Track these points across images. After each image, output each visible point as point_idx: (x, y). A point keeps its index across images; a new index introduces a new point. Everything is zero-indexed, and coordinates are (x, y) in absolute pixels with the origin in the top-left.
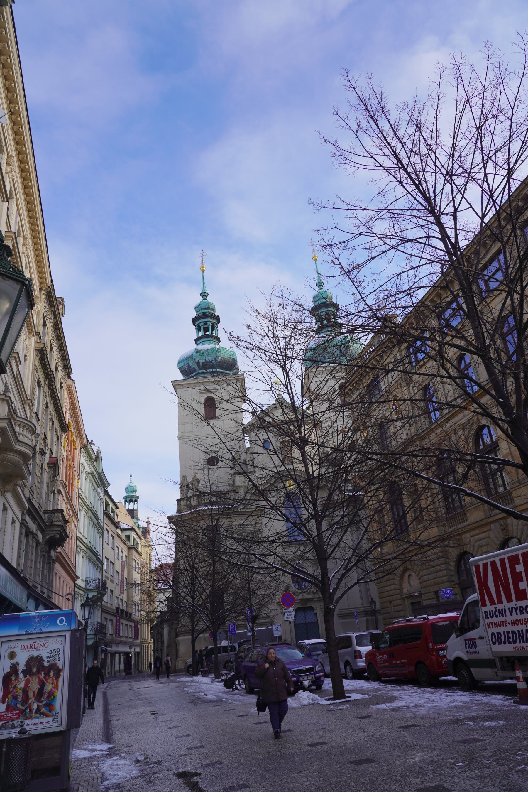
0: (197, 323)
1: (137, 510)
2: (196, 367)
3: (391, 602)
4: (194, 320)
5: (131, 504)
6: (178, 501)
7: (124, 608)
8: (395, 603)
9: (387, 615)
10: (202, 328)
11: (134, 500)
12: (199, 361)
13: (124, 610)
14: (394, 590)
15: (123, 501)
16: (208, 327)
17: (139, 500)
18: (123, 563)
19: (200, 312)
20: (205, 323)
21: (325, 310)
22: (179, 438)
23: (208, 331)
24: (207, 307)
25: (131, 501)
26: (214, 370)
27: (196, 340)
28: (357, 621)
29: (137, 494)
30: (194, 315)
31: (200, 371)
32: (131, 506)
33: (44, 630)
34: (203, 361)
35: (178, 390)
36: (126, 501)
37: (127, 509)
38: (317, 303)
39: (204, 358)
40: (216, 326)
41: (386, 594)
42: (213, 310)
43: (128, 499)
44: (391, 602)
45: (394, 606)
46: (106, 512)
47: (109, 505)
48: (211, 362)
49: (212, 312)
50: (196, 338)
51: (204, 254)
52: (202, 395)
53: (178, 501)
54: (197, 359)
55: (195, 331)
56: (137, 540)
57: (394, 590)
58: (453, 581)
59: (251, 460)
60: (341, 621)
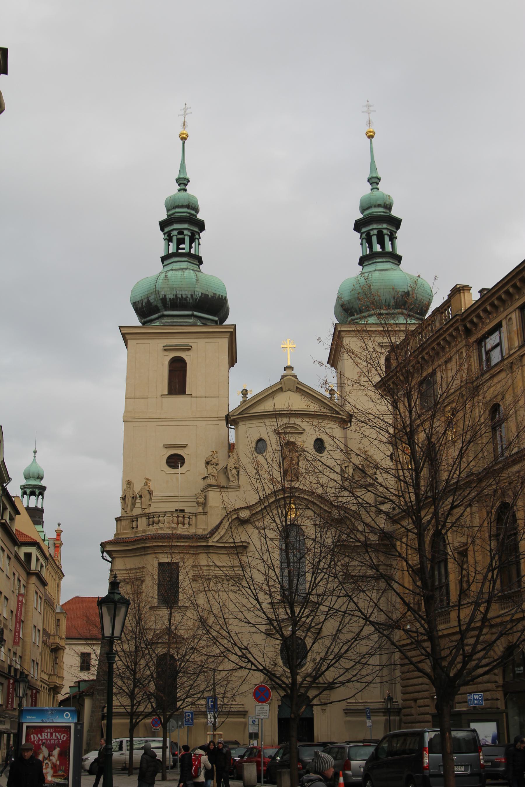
0: (166, 230)
1: (42, 511)
2: (160, 305)
3: (415, 700)
4: (163, 225)
5: (33, 498)
6: (118, 520)
7: (18, 667)
8: (420, 702)
9: (409, 717)
10: (175, 239)
11: (37, 493)
12: (165, 296)
13: (17, 669)
14: (422, 684)
15: (19, 493)
16: (184, 239)
17: (46, 493)
18: (21, 598)
19: (173, 211)
20: (181, 232)
21: (375, 226)
22: (125, 420)
23: (184, 243)
24: (186, 203)
25: (32, 493)
26: (190, 313)
27: (163, 259)
28: (369, 722)
29: (43, 483)
32: (33, 502)
33: (55, 721)
34: (172, 297)
35: (129, 342)
36: (25, 493)
37: (25, 506)
38: (367, 212)
39: (175, 293)
40: (197, 236)
41: (411, 689)
43: (28, 491)
44: (415, 700)
45: (419, 707)
46: (3, 521)
47: (7, 508)
48: (185, 299)
49: (193, 212)
50: (163, 255)
52: (167, 353)
53: (118, 520)
54: (163, 293)
55: (163, 242)
56: (42, 560)
57: (422, 684)
58: (496, 682)
59: (235, 468)
60: (348, 718)
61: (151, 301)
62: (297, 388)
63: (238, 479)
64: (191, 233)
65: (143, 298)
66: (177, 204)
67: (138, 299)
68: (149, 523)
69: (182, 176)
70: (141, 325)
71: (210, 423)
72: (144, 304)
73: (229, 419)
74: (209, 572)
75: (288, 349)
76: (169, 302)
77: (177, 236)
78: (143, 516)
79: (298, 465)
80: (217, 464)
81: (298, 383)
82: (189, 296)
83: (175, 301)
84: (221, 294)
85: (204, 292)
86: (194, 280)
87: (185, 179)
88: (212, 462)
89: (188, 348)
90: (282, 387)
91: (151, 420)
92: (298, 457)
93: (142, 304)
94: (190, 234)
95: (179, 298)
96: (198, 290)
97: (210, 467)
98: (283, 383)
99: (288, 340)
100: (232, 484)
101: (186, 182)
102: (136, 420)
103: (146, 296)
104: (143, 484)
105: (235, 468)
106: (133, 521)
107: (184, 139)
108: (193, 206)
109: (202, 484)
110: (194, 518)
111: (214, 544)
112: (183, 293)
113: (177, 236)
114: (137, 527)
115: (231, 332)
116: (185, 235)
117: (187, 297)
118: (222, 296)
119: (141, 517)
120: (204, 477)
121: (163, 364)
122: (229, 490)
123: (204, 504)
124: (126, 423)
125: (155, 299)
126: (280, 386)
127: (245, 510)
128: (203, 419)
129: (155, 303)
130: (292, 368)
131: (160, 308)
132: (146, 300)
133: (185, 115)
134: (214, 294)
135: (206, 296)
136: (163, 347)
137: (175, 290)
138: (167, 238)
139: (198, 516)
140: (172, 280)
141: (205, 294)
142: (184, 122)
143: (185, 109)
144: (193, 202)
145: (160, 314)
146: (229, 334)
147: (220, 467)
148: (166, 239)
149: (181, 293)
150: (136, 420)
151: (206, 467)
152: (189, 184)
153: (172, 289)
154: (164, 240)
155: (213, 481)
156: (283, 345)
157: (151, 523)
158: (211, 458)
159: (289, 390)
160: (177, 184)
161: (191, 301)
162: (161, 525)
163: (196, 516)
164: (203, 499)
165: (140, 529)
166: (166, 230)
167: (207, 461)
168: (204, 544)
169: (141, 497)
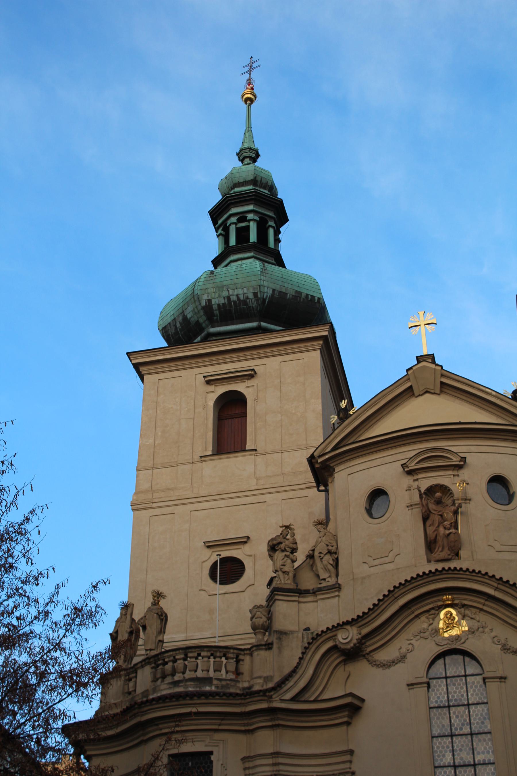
0: (220, 222)
2: (202, 319)
12: (210, 301)
20: (242, 218)
22: (136, 507)
26: (254, 324)
27: (216, 262)
30: (217, 198)
31: (213, 330)
34: (222, 301)
39: (225, 294)
42: (272, 188)
48: (245, 302)
51: (254, 65)
52: (211, 388)
54: (205, 297)
59: (330, 552)
61: (189, 316)
62: (442, 383)
63: (337, 575)
64: (259, 217)
65: (176, 316)
66: (236, 180)
67: (169, 320)
68: (155, 674)
69: (246, 146)
70: (166, 345)
71: (291, 494)
72: (178, 325)
73: (317, 466)
74: (276, 768)
75: (423, 326)
76: (217, 312)
77: (236, 224)
78: (146, 664)
79: (457, 528)
80: (294, 550)
81: (442, 375)
82: (251, 296)
83: (227, 308)
84: (311, 293)
85: (278, 288)
86: (259, 269)
87: (250, 149)
88: (282, 546)
89: (251, 375)
90: (411, 387)
91: (182, 501)
92: (456, 512)
93: (175, 326)
94: (258, 219)
95: (235, 302)
96: (266, 284)
97: (279, 556)
98: (412, 378)
99: (421, 313)
100: (324, 584)
101: (253, 155)
102: (155, 505)
103: (181, 311)
104: (150, 605)
105: (330, 552)
106: (130, 680)
107: (249, 101)
108: (264, 181)
109: (268, 592)
110: (247, 658)
111: (283, 705)
112: (240, 291)
113: (236, 224)
114: (135, 691)
115: (324, 338)
116: (249, 221)
117: (247, 298)
118: (313, 297)
119: (142, 667)
120: (268, 579)
121: (204, 407)
122: (319, 597)
123: (267, 628)
124: (137, 512)
125: (193, 311)
126: (408, 385)
127: (348, 627)
128: (278, 489)
129: (195, 318)
130: (432, 357)
131: (204, 325)
132: (181, 318)
133: (250, 72)
134: (297, 292)
135: (283, 295)
136: (204, 377)
137: (225, 289)
138: (222, 232)
139: (255, 654)
140: (221, 276)
141: (280, 292)
142: (250, 79)
143: (252, 62)
144: (262, 175)
145: (203, 335)
146: (321, 342)
147: (301, 557)
148: (220, 234)
149: (236, 292)
150: (155, 505)
151: (271, 556)
152: (259, 160)
153: (220, 288)
154: (218, 236)
155: (286, 582)
156: (412, 322)
157: (159, 675)
158: (280, 539)
159: (427, 392)
160: (240, 162)
161: (255, 304)
162: (177, 678)
163: (251, 655)
164: (264, 619)
165: (139, 690)
166: (220, 222)
167: (271, 544)
168: (264, 705)
169: (144, 628)
